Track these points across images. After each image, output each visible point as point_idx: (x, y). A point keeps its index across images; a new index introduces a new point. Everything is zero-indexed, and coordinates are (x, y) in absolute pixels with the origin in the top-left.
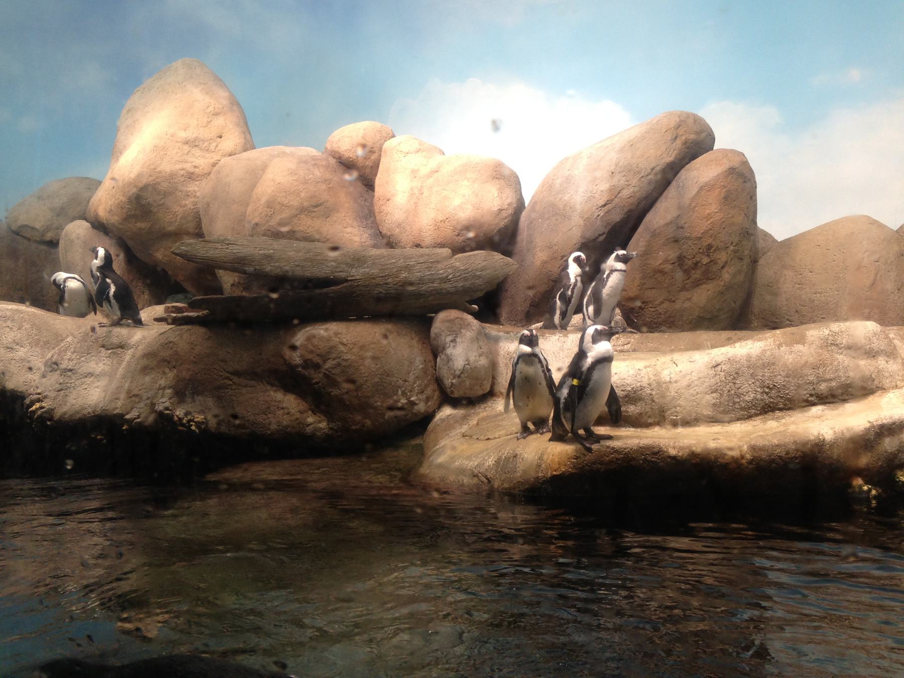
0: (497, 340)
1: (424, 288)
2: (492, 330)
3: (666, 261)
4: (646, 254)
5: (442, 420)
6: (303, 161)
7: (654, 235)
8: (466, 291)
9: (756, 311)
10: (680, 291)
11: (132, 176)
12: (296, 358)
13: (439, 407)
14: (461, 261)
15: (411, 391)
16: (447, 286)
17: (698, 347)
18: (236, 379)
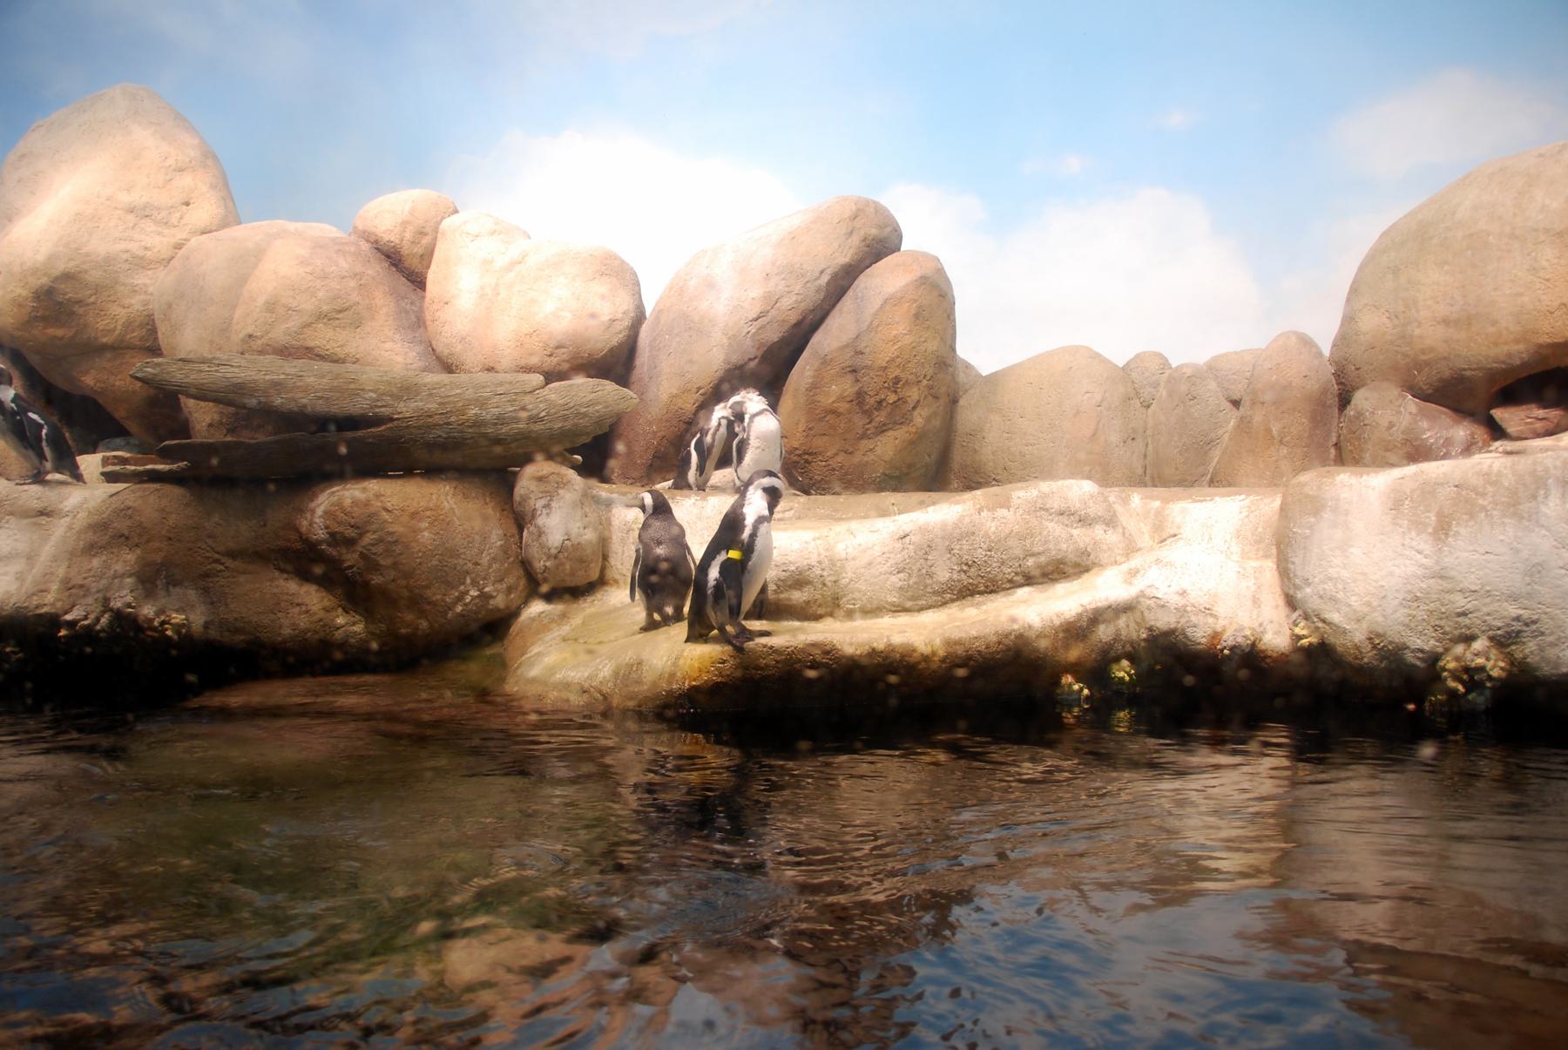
0: (609, 504)
2: (602, 491)
3: (841, 398)
5: (533, 619)
6: (318, 245)
7: (825, 362)
8: (563, 435)
9: (955, 466)
11: (41, 257)
12: (321, 534)
13: (526, 602)
16: (537, 427)
17: (884, 513)
18: (229, 562)
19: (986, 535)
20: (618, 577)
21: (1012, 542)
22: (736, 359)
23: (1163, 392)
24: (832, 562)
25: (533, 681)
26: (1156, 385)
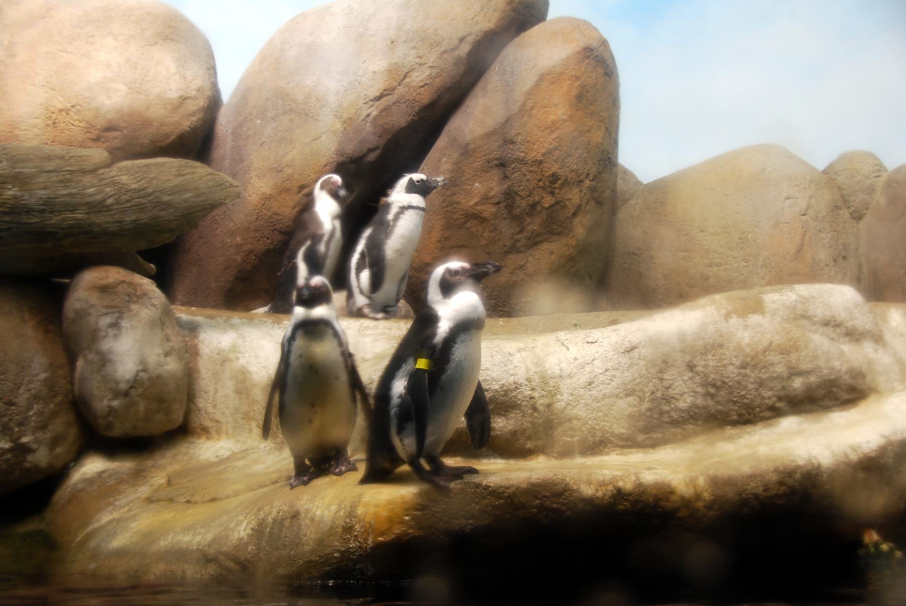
0: (193, 329)
1: (55, 220)
3: (485, 199)
4: (453, 184)
5: (90, 481)
7: (467, 152)
8: (139, 230)
10: (508, 252)
13: (78, 456)
14: (130, 175)
15: (21, 424)
16: (102, 219)
19: (739, 348)
20: (208, 424)
21: (772, 357)
22: (351, 149)
23: (880, 199)
24: (544, 380)
25: (121, 553)
26: (871, 190)
